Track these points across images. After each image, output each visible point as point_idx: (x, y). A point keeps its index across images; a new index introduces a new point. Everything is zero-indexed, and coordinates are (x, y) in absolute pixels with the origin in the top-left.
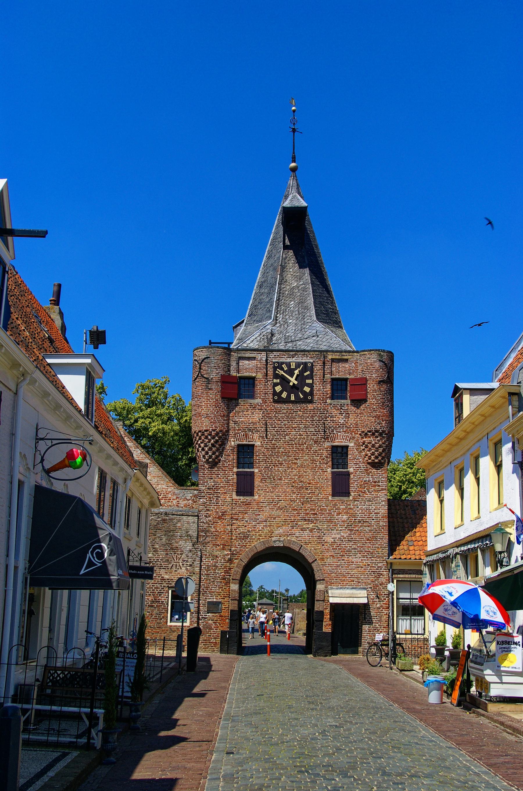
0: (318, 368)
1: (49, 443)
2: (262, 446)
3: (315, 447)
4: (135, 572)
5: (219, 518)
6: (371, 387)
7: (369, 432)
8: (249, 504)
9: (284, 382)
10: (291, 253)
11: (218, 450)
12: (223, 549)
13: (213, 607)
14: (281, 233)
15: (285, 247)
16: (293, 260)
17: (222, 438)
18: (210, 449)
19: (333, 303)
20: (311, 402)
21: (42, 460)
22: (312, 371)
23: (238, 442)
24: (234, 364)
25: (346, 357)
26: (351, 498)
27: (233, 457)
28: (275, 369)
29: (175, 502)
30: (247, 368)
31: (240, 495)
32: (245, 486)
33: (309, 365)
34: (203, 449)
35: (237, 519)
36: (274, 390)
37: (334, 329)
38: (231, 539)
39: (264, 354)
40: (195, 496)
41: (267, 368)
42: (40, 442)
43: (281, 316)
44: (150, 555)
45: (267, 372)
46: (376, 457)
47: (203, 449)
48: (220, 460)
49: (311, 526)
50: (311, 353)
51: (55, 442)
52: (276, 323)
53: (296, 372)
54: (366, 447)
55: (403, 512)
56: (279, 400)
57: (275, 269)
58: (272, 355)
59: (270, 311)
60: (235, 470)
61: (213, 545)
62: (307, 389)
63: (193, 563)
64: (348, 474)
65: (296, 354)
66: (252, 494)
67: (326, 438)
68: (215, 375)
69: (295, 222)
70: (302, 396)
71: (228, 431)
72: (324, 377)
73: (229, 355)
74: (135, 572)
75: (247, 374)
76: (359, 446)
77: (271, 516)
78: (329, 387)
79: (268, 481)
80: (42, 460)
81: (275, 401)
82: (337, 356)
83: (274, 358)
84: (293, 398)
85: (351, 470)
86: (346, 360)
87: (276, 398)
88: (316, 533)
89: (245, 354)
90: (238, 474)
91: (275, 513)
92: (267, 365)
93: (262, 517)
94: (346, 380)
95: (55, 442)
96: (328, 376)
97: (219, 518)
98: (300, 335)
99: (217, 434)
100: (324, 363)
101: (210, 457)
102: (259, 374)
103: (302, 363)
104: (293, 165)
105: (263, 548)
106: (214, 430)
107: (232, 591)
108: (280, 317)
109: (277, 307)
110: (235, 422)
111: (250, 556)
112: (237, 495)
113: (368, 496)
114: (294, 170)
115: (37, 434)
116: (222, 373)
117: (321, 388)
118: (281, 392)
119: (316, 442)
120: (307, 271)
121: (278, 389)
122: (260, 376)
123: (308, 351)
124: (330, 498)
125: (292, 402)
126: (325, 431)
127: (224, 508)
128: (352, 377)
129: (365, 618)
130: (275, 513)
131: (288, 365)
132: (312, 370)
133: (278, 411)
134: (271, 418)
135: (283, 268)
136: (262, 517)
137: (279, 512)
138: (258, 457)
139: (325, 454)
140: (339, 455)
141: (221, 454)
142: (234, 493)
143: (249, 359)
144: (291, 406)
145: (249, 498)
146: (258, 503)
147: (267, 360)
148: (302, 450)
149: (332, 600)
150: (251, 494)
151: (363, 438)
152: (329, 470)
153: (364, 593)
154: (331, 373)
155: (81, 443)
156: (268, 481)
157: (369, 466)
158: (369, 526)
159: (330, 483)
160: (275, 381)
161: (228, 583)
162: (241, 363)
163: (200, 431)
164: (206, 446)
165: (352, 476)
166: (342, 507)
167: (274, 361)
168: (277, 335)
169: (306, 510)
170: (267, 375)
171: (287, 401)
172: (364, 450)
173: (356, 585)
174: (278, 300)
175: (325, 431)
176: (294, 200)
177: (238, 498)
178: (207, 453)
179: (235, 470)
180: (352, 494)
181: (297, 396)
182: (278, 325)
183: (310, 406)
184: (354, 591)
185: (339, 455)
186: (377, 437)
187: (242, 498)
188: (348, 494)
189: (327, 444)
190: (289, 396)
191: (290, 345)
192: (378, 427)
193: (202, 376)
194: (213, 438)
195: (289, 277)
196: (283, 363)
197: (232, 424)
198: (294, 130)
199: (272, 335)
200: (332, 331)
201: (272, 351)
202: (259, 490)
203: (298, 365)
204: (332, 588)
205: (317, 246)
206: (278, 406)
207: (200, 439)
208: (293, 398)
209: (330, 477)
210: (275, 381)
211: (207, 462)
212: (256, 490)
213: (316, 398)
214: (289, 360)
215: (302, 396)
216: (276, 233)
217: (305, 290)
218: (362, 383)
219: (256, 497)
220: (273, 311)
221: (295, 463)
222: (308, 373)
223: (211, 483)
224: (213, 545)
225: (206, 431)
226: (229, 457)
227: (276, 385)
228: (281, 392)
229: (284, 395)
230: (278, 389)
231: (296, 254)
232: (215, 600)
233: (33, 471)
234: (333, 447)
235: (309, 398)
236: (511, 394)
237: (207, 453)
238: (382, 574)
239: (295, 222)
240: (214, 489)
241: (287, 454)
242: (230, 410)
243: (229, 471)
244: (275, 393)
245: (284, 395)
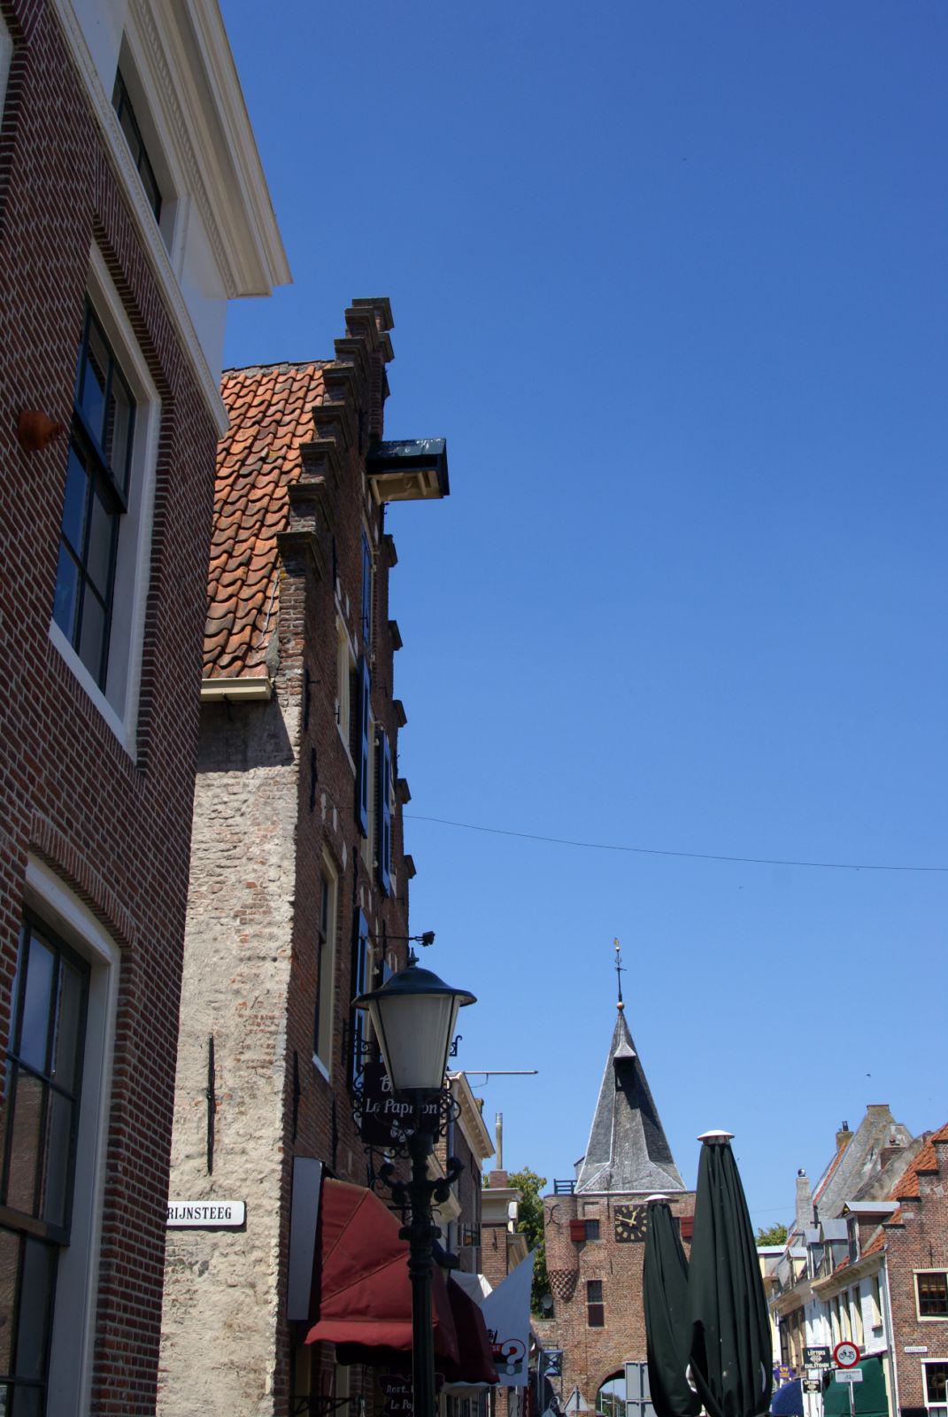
5: (575, 1346)
8: (600, 1333)
9: (624, 1224)
10: (623, 1095)
11: (571, 1286)
14: (614, 1074)
15: (618, 1089)
16: (625, 1102)
17: (574, 1276)
18: (564, 1286)
19: (663, 1139)
24: (580, 1209)
30: (592, 1212)
32: (596, 1317)
36: (617, 1232)
37: (665, 1167)
39: (606, 1198)
40: (553, 1327)
53: (634, 1214)
57: (609, 1111)
58: (612, 1199)
59: (608, 1153)
60: (587, 1303)
68: (565, 1220)
69: (628, 1075)
71: (578, 1270)
73: (576, 1201)
75: (591, 1217)
77: (619, 1343)
81: (617, 1241)
83: (614, 1202)
84: (633, 1237)
86: (677, 1201)
89: (588, 1199)
90: (590, 1307)
91: (624, 1340)
94: (678, 1218)
97: (575, 1346)
99: (570, 1273)
104: (620, 1004)
109: (614, 1147)
114: (621, 1008)
116: (570, 1218)
118: (622, 1233)
120: (638, 1112)
122: (603, 1219)
125: (633, 1241)
127: (579, 1338)
128: (682, 1216)
130: (624, 1340)
131: (627, 1207)
133: (620, 1250)
134: (614, 1256)
135: (617, 1109)
138: (606, 1291)
141: (574, 1290)
143: (592, 1203)
144: (631, 1245)
145: (600, 1328)
150: (601, 1323)
162: (588, 1208)
170: (609, 1217)
171: (628, 1240)
174: (614, 1142)
176: (624, 1051)
179: (587, 1303)
181: (636, 1236)
190: (629, 1236)
195: (623, 1119)
197: (581, 1263)
198: (619, 969)
199: (611, 1176)
200: (664, 1170)
203: (635, 1207)
205: (646, 1084)
206: (620, 1245)
208: (633, 1237)
214: (627, 1203)
216: (608, 1073)
217: (637, 1131)
219: (606, 1327)
223: (566, 1316)
226: (581, 1294)
227: (617, 1226)
228: (622, 1233)
229: (625, 1235)
230: (620, 1229)
231: (627, 1095)
236: (773, 1281)
239: (628, 1075)
240: (568, 1322)
241: (630, 1287)
242: (579, 1250)
243: (581, 1305)
245: (625, 1235)
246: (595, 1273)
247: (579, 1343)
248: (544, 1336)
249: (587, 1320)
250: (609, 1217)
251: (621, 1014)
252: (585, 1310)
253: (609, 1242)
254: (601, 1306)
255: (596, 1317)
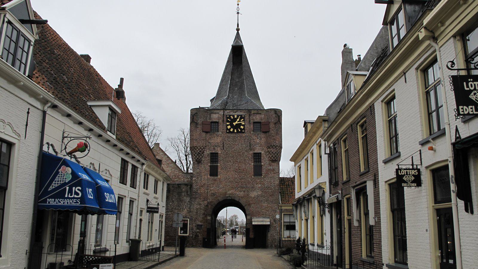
0: (247, 117)
1: (69, 139)
2: (222, 153)
3: (246, 153)
4: (150, 210)
5: (202, 186)
6: (272, 126)
7: (271, 146)
8: (215, 180)
12: (204, 201)
13: (199, 227)
18: (197, 155)
20: (244, 132)
21: (66, 148)
22: (244, 119)
23: (210, 152)
25: (260, 112)
26: (262, 177)
27: (209, 158)
28: (227, 118)
29: (182, 179)
30: (215, 117)
31: (212, 176)
32: (214, 172)
33: (243, 116)
34: (194, 155)
35: (210, 187)
38: (208, 196)
39: (222, 111)
41: (223, 118)
42: (65, 139)
43: (231, 94)
44: (171, 203)
45: (224, 119)
46: (274, 158)
47: (194, 155)
48: (202, 160)
49: (244, 190)
50: (244, 111)
51: (72, 139)
52: (229, 98)
54: (269, 153)
55: (287, 183)
56: (230, 132)
58: (226, 112)
60: (209, 164)
61: (199, 199)
62: (242, 127)
63: (190, 207)
64: (261, 166)
65: (237, 111)
66: (217, 175)
67: (251, 149)
70: (240, 130)
72: (250, 122)
74: (150, 210)
75: (215, 120)
76: (266, 153)
77: (226, 185)
78: (252, 126)
79: (225, 169)
80: (66, 148)
81: (227, 133)
82: (256, 112)
84: (235, 131)
85: (262, 164)
87: (228, 131)
88: (246, 192)
90: (210, 166)
92: (223, 116)
93: (221, 186)
95: (72, 139)
96: (252, 121)
97: (202, 186)
98: (239, 103)
99: (201, 148)
100: (250, 115)
101: (198, 158)
102: (220, 120)
103: (240, 115)
105: (222, 199)
106: (199, 146)
107: (208, 219)
108: (231, 95)
110: (209, 143)
111: (216, 204)
112: (210, 176)
113: (270, 175)
115: (63, 135)
117: (249, 127)
118: (230, 129)
119: (246, 151)
121: (229, 127)
122: (221, 121)
123: (243, 110)
124: (253, 177)
126: (250, 146)
129: (269, 232)
131: (234, 116)
132: (244, 118)
133: (229, 137)
134: (225, 140)
136: (221, 186)
137: (229, 184)
138: (220, 158)
139: (250, 156)
140: (257, 157)
142: (209, 175)
146: (220, 179)
147: (223, 114)
148: (240, 155)
149: (253, 223)
150: (216, 175)
151: (267, 149)
152: (252, 164)
153: (269, 220)
154: (253, 119)
155: (85, 139)
156: (225, 169)
157: (270, 162)
158: (271, 189)
159: (253, 170)
160: (227, 123)
161: (206, 216)
163: (193, 147)
164: (196, 154)
165: (263, 167)
166: (258, 181)
167: (227, 114)
168: (229, 103)
169: (242, 182)
172: (268, 154)
173: (264, 216)
175: (250, 146)
177: (211, 177)
178: (196, 157)
179: (209, 164)
180: (263, 175)
181: (237, 130)
182: (230, 98)
183: (244, 135)
184: (264, 219)
185: (257, 157)
186: (274, 148)
187: (212, 177)
188: (261, 175)
189: (251, 152)
190: (234, 130)
191: (235, 107)
192: (275, 144)
193: (194, 121)
194: (199, 150)
196: (231, 115)
201: (226, 110)
202: (220, 173)
204: (254, 218)
206: (229, 135)
207: (193, 150)
208: (235, 131)
209: (253, 167)
210: (227, 123)
211: (196, 161)
212: (219, 173)
213: (246, 131)
214: (234, 114)
215: (240, 130)
218: (268, 124)
219: (219, 177)
220: (228, 93)
221: (237, 161)
222: (243, 120)
224: (199, 199)
225: (196, 146)
227: (228, 125)
228: (230, 129)
229: (232, 130)
230: (229, 127)
232: (200, 224)
233: (61, 153)
234: (254, 153)
235: (243, 131)
237: (196, 157)
238: (276, 211)
241: (233, 157)
244: (227, 129)
245: (232, 130)
246: (214, 148)
247: (204, 184)
248: (187, 181)
249: (209, 173)
250: (223, 121)
251: (238, 33)
252: (208, 168)
253: (222, 133)
254: (217, 166)
255: (214, 172)
